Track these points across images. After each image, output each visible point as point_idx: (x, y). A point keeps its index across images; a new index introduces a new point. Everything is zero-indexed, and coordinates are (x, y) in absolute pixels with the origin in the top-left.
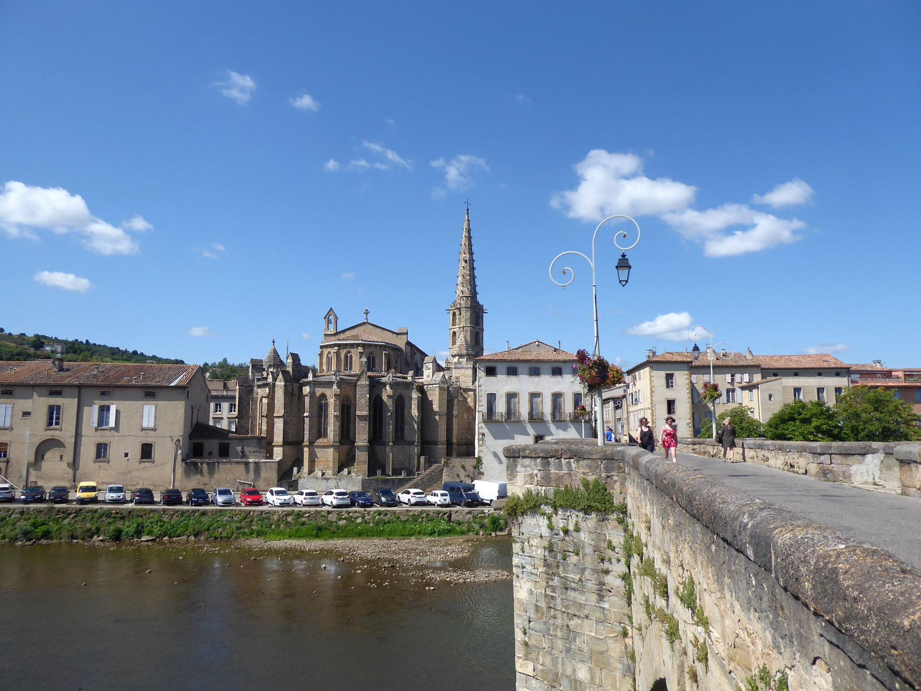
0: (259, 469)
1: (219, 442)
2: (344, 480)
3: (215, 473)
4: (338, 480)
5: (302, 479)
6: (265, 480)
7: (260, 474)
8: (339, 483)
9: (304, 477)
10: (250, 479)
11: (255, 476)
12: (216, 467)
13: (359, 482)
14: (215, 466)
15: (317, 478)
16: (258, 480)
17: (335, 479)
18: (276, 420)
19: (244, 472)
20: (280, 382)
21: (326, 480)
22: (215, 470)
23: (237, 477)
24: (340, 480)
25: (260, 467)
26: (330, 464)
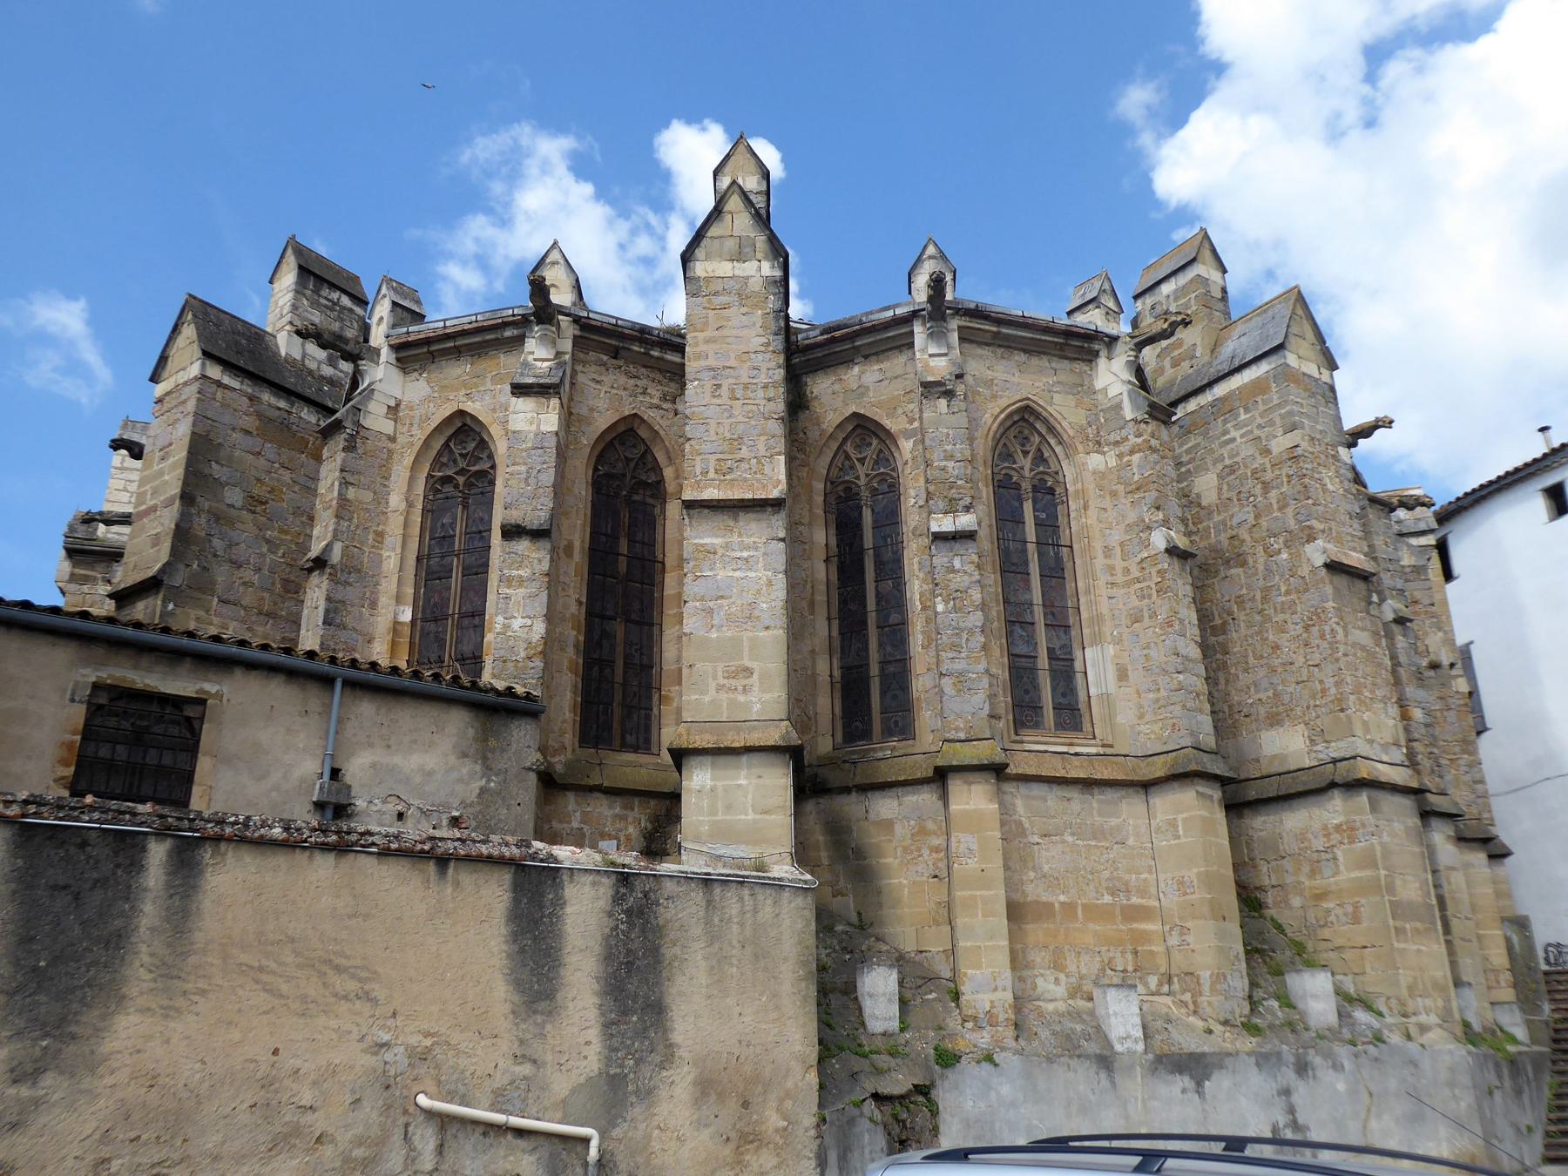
0: (654, 952)
1: (91, 675)
2: (1337, 1067)
3: (110, 994)
4: (1289, 1076)
5: (969, 1075)
6: (706, 1087)
7: (656, 1011)
8: (1296, 1099)
9: (989, 1058)
10: (561, 1085)
11: (608, 1061)
12: (150, 912)
13: (1451, 1084)
14: (129, 895)
15: (1106, 1061)
16: (647, 1094)
17: (1264, 1060)
18: (701, 536)
19: (501, 994)
20: (739, 257)
21: (1186, 1081)
22: (117, 942)
23: (421, 1056)
24: (1302, 1068)
25: (659, 931)
26: (1145, 937)
